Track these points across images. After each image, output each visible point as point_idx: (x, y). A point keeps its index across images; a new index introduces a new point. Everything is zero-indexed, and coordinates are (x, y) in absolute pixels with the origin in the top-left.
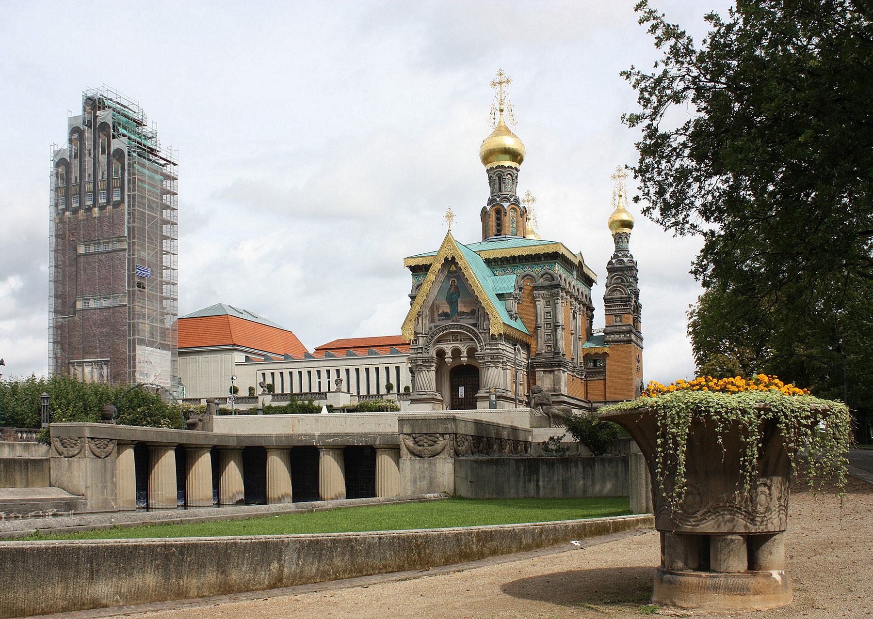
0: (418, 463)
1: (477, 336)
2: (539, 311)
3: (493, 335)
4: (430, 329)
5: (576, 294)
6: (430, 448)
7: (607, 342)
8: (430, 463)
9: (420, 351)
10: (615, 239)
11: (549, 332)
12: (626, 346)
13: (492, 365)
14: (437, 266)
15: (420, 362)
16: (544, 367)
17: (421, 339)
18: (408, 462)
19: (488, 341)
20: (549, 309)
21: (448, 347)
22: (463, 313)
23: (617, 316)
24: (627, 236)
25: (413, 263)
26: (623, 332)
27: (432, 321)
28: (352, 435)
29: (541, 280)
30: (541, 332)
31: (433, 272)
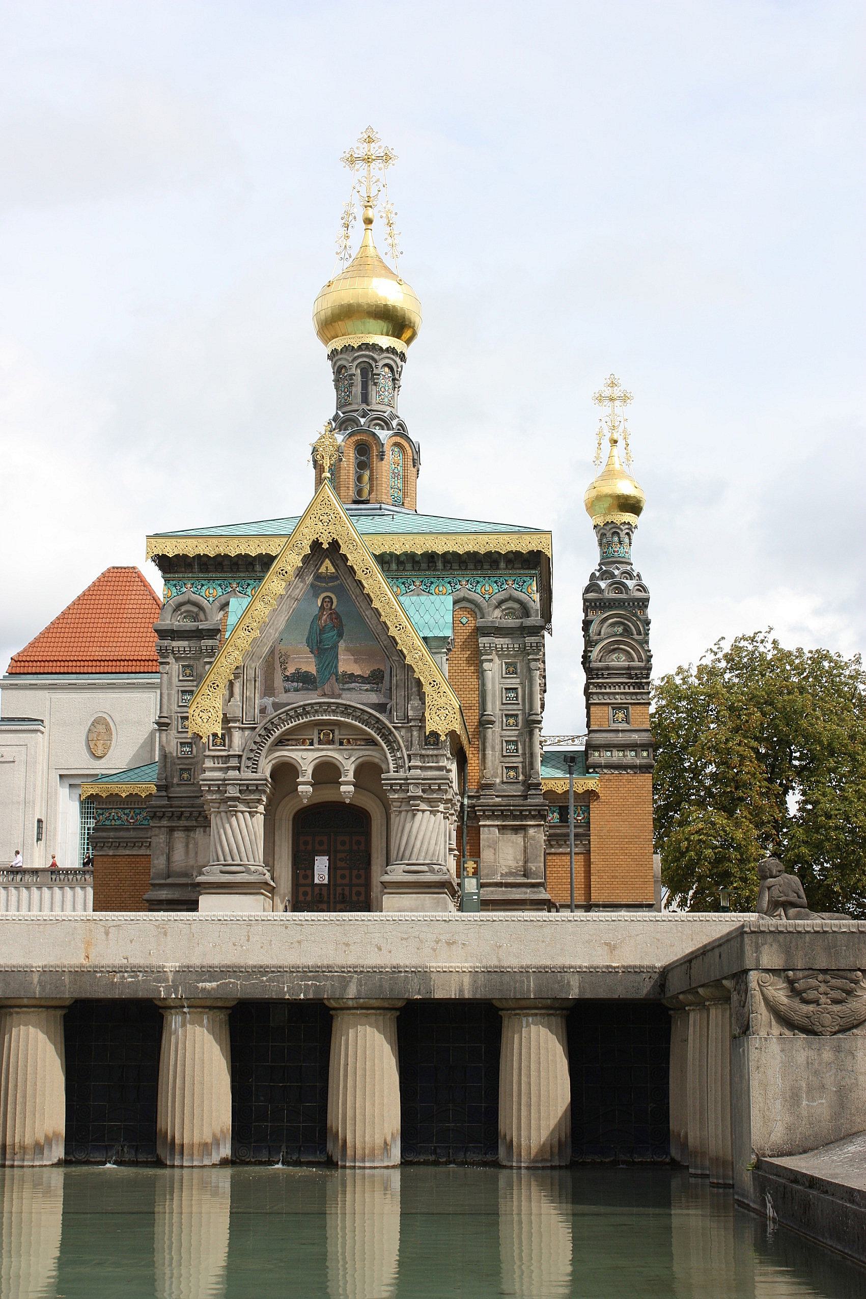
0: (802, 1049)
1: (387, 735)
2: (489, 686)
3: (434, 734)
4: (263, 711)
6: (836, 1008)
7: (596, 767)
8: (838, 1050)
9: (234, 762)
11: (512, 734)
13: (423, 806)
14: (292, 560)
15: (233, 792)
16: (503, 817)
17: (237, 736)
18: (774, 1047)
19: (416, 749)
20: (514, 682)
21: (306, 759)
22: (352, 678)
23: (617, 707)
24: (631, 527)
25: (171, 549)
26: (633, 746)
27: (269, 690)
28: (279, 972)
29: (497, 613)
30: (494, 734)
31: (283, 573)
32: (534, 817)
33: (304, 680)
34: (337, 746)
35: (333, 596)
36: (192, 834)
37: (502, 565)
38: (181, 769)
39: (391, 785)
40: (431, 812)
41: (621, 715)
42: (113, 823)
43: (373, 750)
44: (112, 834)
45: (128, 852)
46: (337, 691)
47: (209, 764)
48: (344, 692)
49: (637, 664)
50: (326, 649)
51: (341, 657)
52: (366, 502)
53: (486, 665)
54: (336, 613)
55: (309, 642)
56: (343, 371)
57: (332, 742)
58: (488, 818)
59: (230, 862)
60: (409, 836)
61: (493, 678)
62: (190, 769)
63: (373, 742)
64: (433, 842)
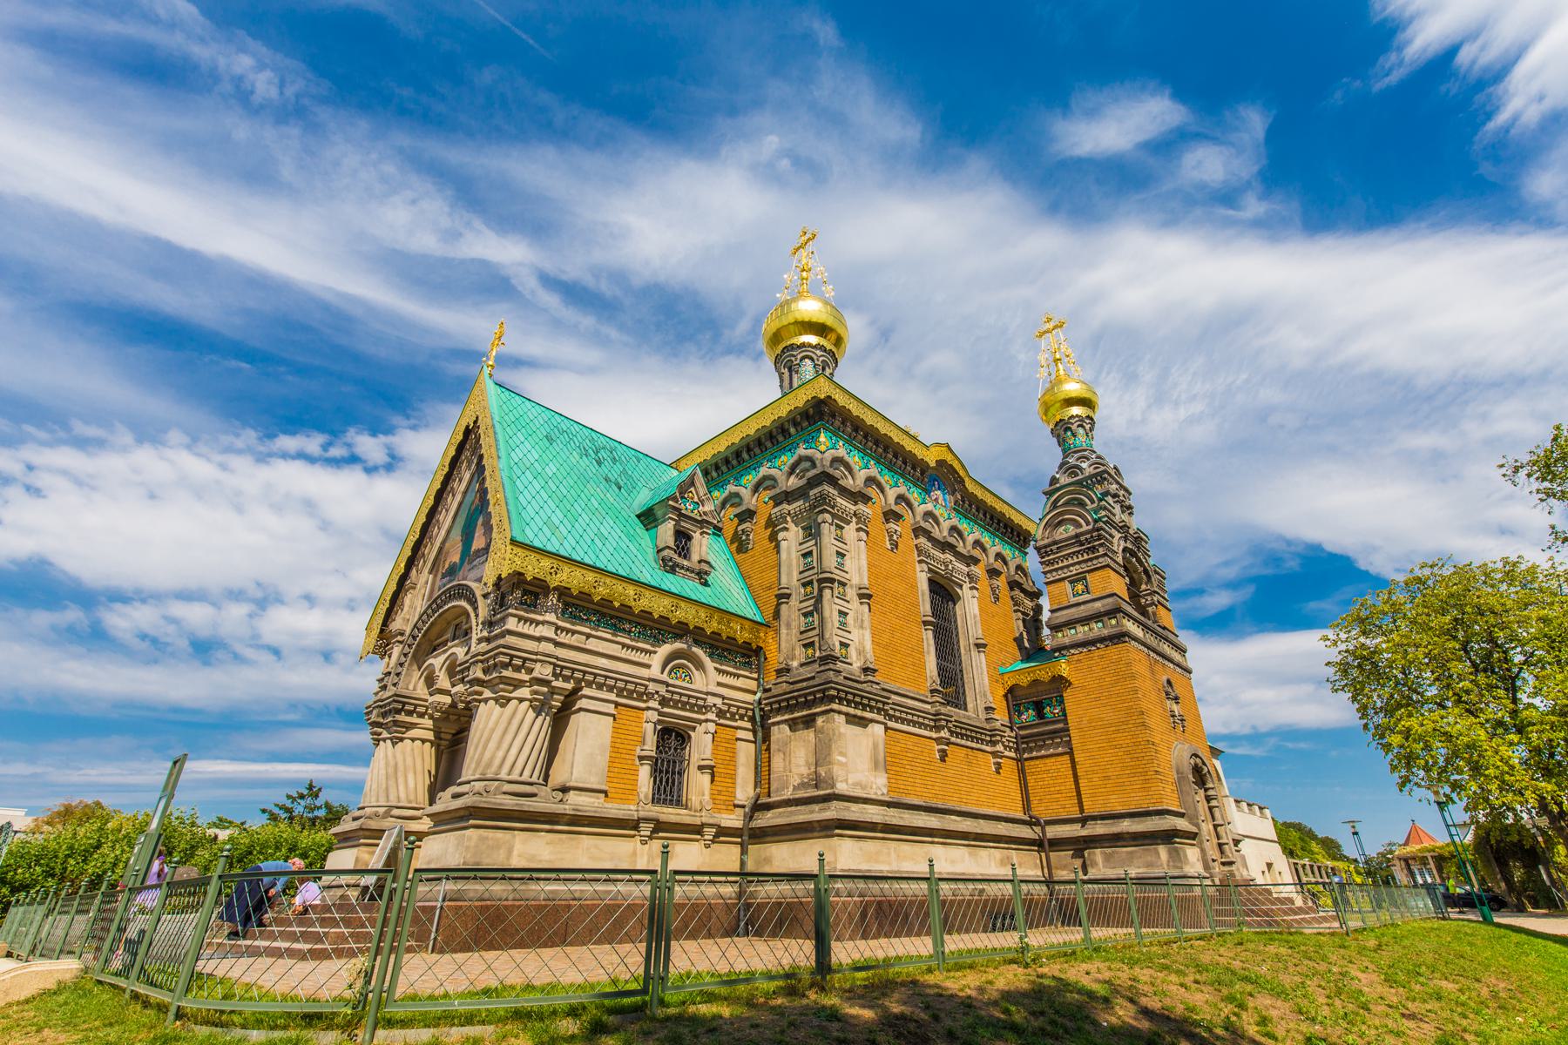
5: (941, 533)
10: (1058, 436)
12: (1113, 651)
16: (790, 709)
26: (1097, 617)
30: (792, 612)
32: (822, 701)
37: (792, 430)
40: (496, 700)
41: (1080, 587)
49: (1085, 528)
53: (781, 535)
58: (779, 711)
61: (789, 548)
64: (492, 745)
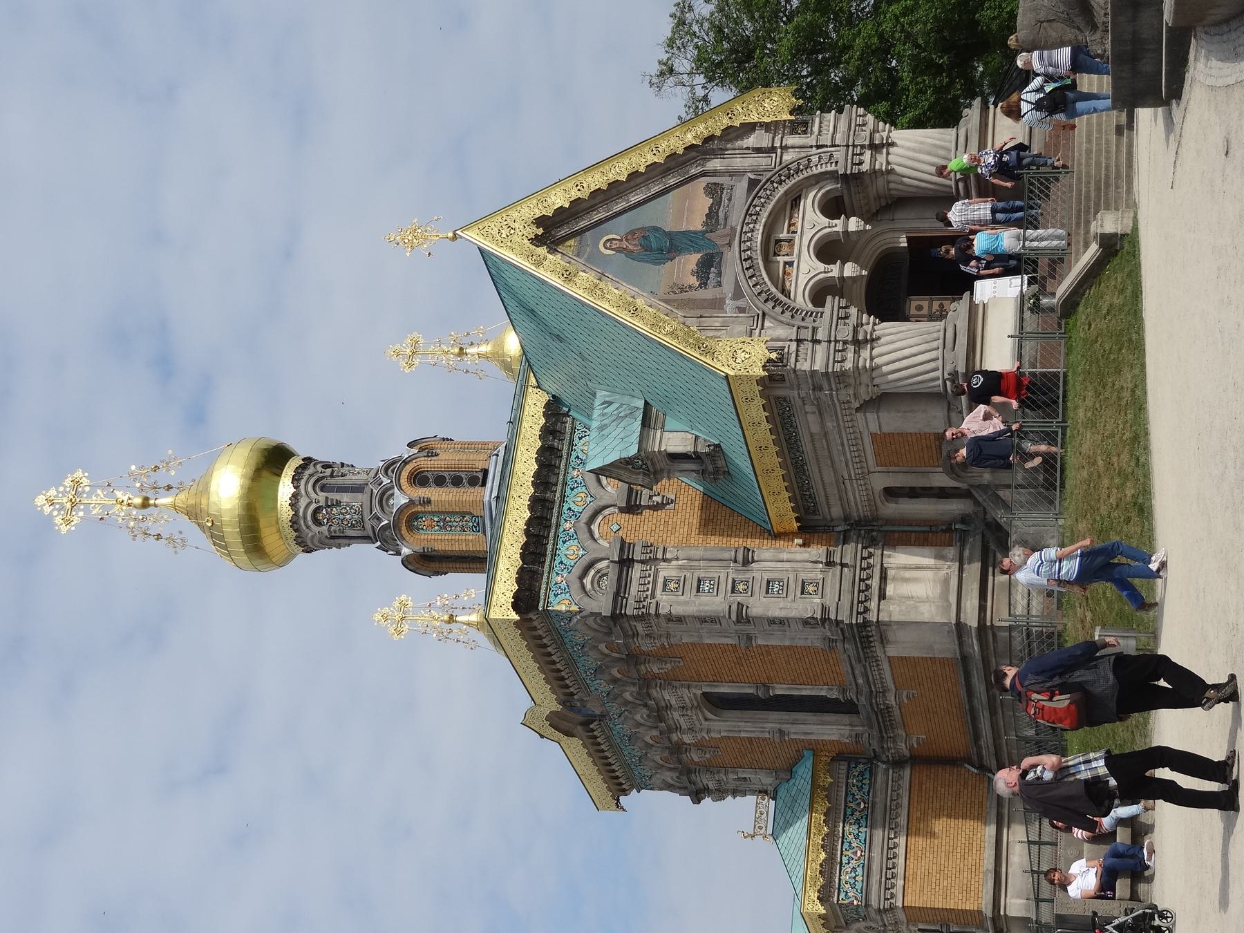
4: (742, 310)
22: (712, 215)
27: (717, 304)
33: (708, 266)
34: (797, 236)
35: (605, 239)
36: (891, 573)
38: (802, 593)
39: (853, 164)
42: (859, 878)
43: (806, 198)
44: (875, 879)
45: (901, 861)
46: (727, 230)
47: (805, 366)
48: (729, 224)
50: (671, 244)
51: (684, 228)
52: (486, 472)
54: (627, 234)
55: (659, 264)
56: (320, 517)
57: (790, 241)
59: (941, 341)
60: (920, 151)
62: (803, 583)
63: (795, 200)
